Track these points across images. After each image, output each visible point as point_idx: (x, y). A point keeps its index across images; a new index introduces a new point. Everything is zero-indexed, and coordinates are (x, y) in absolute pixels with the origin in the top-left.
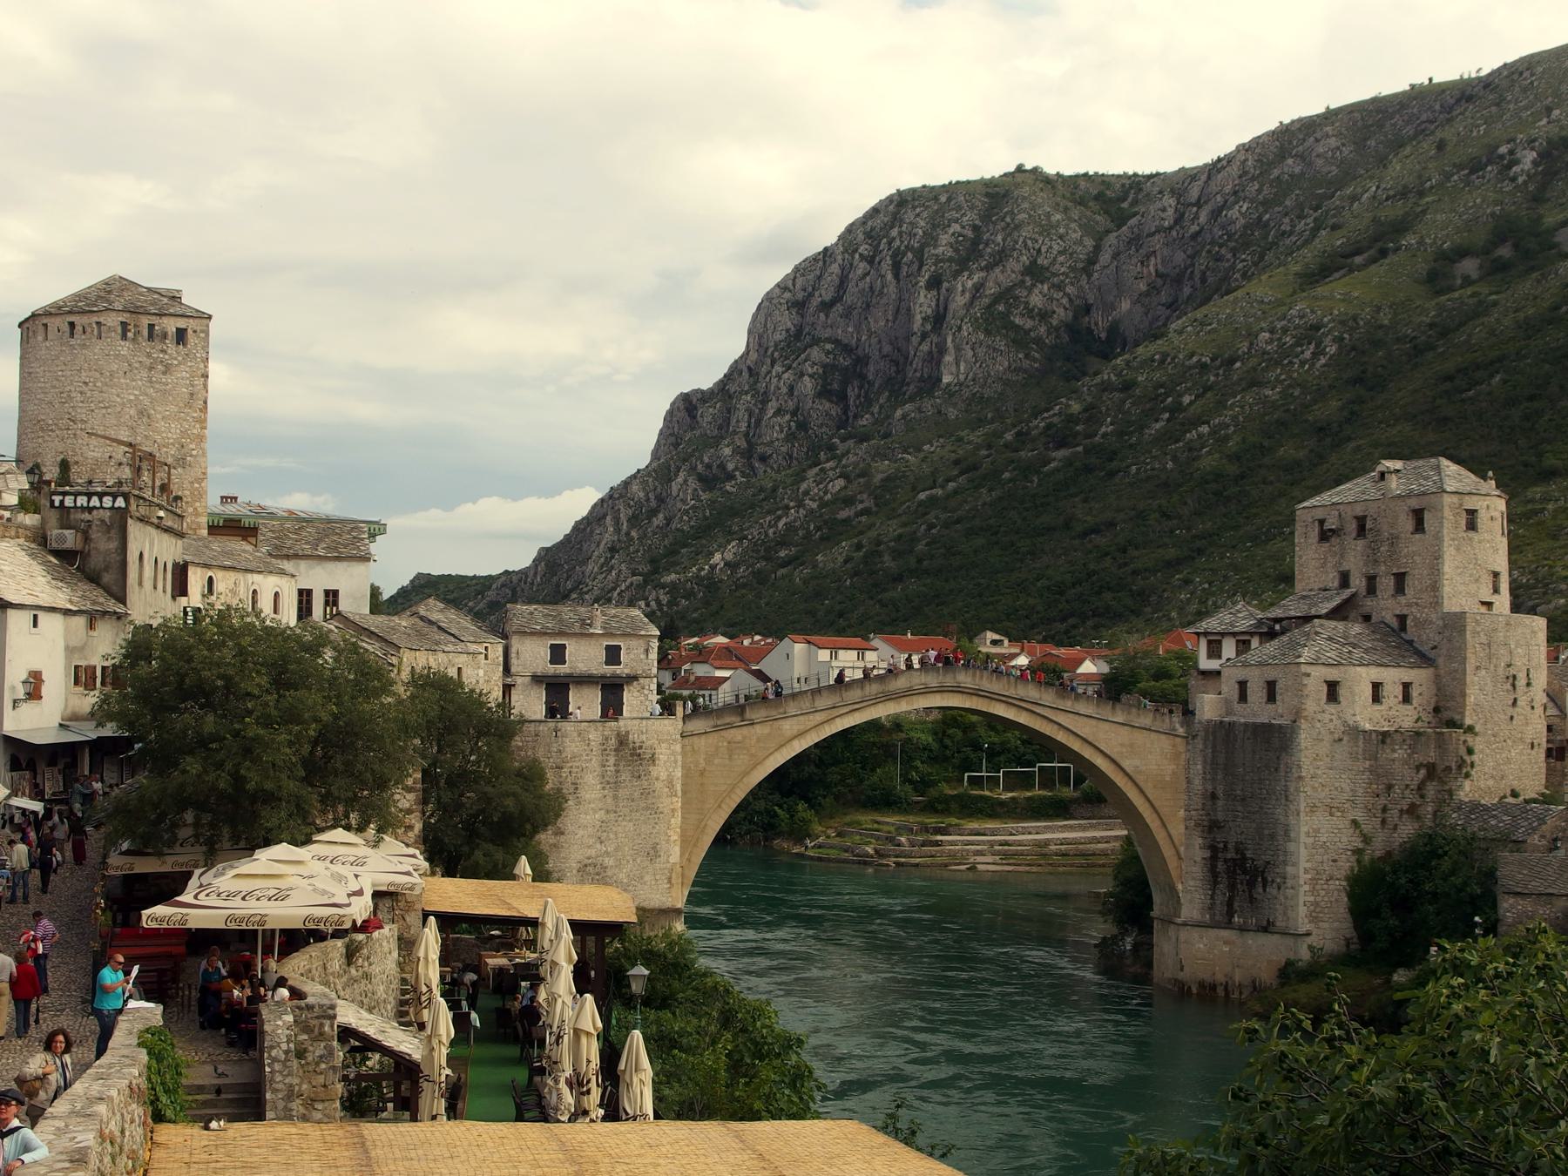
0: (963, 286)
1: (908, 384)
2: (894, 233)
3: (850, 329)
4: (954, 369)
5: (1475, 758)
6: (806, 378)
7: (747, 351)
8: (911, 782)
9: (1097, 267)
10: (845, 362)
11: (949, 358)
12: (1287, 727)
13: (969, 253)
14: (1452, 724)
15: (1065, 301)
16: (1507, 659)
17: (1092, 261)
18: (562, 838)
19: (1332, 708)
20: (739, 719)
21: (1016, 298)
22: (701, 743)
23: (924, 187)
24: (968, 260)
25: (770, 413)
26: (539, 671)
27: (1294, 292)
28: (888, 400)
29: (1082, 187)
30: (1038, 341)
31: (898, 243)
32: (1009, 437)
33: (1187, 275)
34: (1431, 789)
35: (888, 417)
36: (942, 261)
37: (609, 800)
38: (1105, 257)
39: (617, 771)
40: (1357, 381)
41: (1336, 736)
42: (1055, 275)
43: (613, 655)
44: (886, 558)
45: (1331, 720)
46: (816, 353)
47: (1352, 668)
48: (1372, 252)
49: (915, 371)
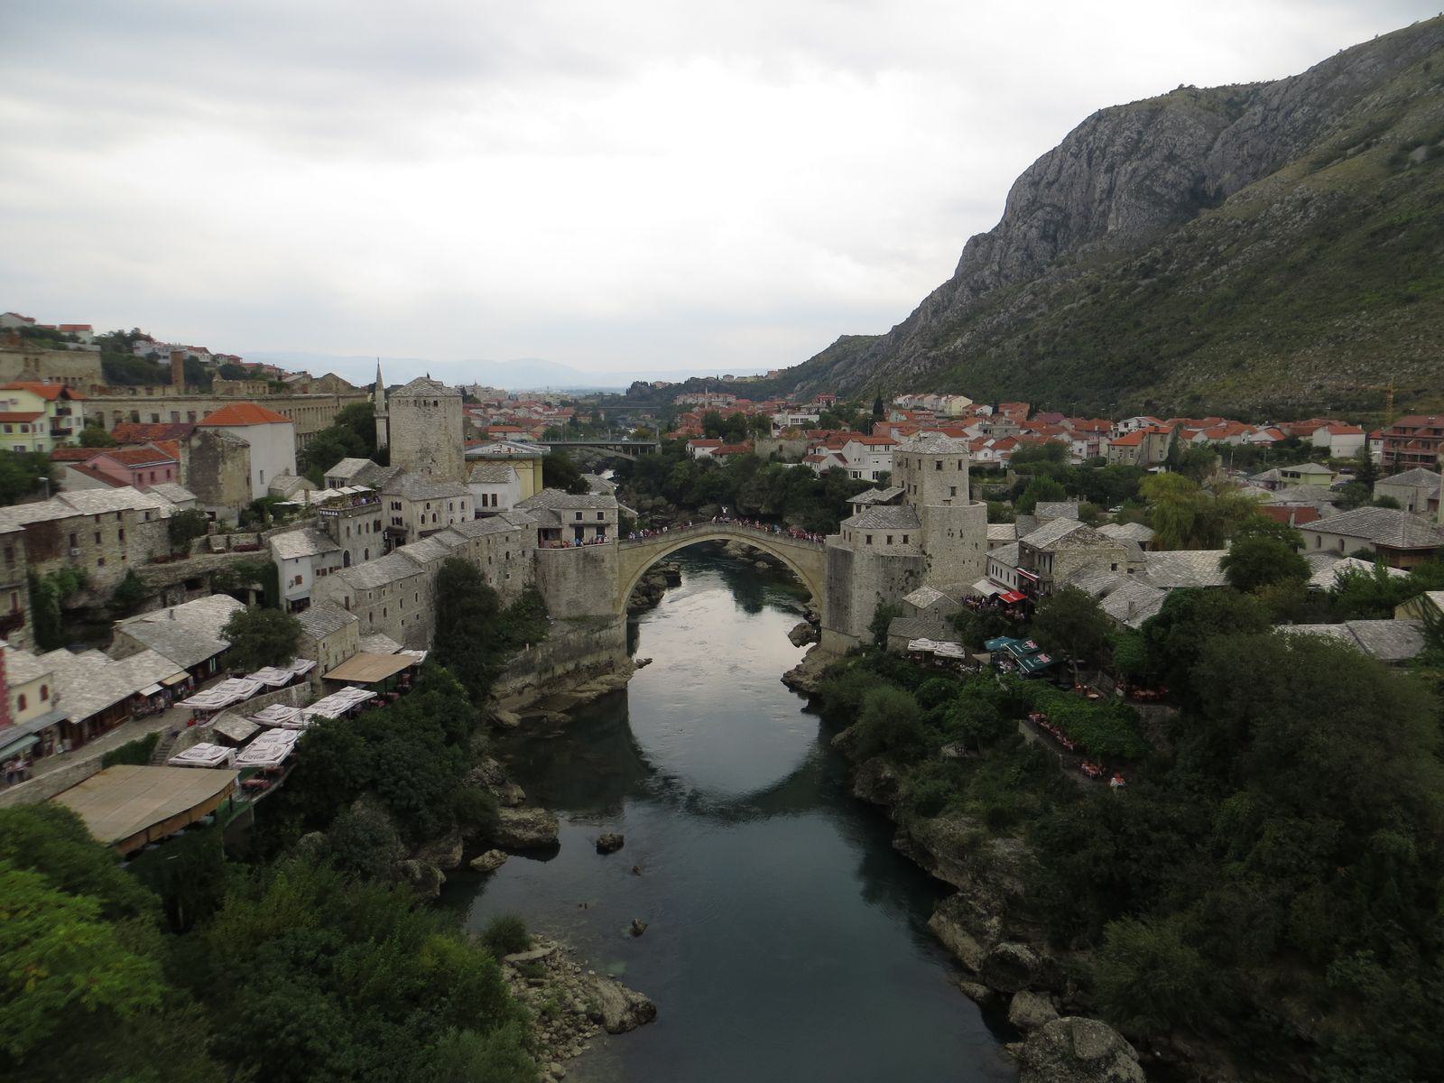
0: (1126, 170)
2: (1091, 138)
4: (1115, 222)
6: (1034, 229)
7: (1005, 213)
10: (1058, 217)
11: (1112, 216)
12: (850, 553)
13: (1132, 150)
14: (924, 553)
15: (1189, 175)
16: (949, 526)
19: (869, 546)
23: (1115, 106)
24: (1131, 153)
25: (1012, 250)
26: (572, 523)
27: (1304, 175)
28: (1078, 240)
29: (1219, 96)
30: (1170, 202)
31: (1090, 147)
33: (1265, 156)
34: (911, 579)
36: (1117, 155)
38: (1217, 146)
39: (585, 567)
40: (1323, 235)
42: (1183, 159)
43: (600, 516)
46: (1040, 213)
48: (1362, 145)
49: (1095, 223)
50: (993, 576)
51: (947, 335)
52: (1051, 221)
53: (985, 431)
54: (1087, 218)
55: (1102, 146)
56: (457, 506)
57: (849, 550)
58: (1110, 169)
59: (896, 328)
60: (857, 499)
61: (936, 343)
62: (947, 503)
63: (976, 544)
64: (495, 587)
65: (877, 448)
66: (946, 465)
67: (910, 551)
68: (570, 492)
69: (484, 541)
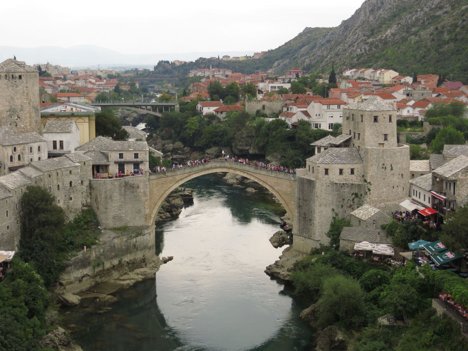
5: (371, 191)
12: (313, 181)
14: (365, 181)
18: (107, 210)
19: (326, 176)
20: (164, 175)
22: (154, 182)
34: (356, 200)
37: (122, 199)
41: (328, 185)
43: (136, 156)
44: (445, 34)
45: (326, 180)
47: (332, 165)
50: (414, 197)
51: (381, 27)
53: (408, 95)
56: (35, 149)
57: (312, 179)
59: (344, 22)
60: (318, 143)
61: (372, 33)
62: (382, 145)
63: (402, 175)
64: (62, 206)
65: (331, 107)
66: (380, 118)
67: (355, 179)
68: (115, 139)
69: (54, 174)
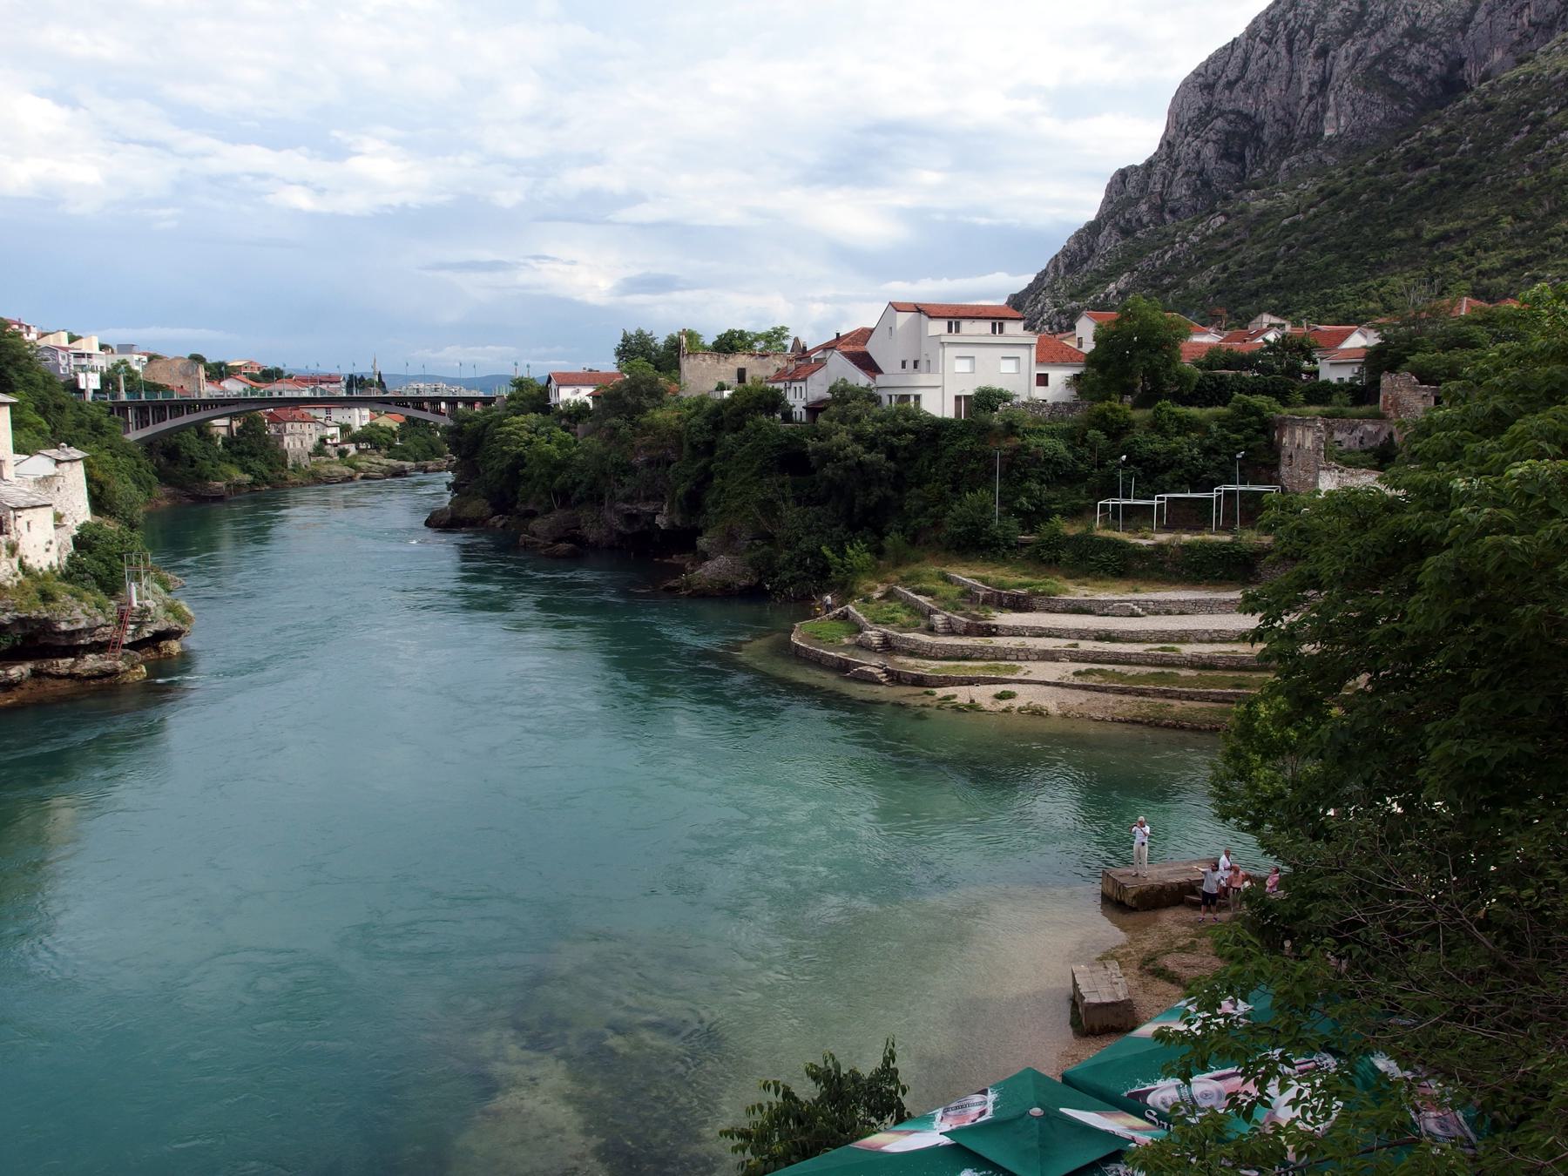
0: (1347, 51)
1: (1296, 141)
3: (1250, 101)
4: (1334, 124)
8: (1020, 512)
9: (1472, 24)
10: (1244, 128)
11: (1330, 114)
15: (1440, 57)
17: (1467, 20)
21: (1395, 58)
24: (1353, 30)
28: (1278, 155)
32: (1370, 164)
35: (1276, 170)
38: (1480, 16)
49: (1302, 129)
52: (1234, 133)
54: (1288, 127)
55: (1308, 23)
58: (1323, 53)
